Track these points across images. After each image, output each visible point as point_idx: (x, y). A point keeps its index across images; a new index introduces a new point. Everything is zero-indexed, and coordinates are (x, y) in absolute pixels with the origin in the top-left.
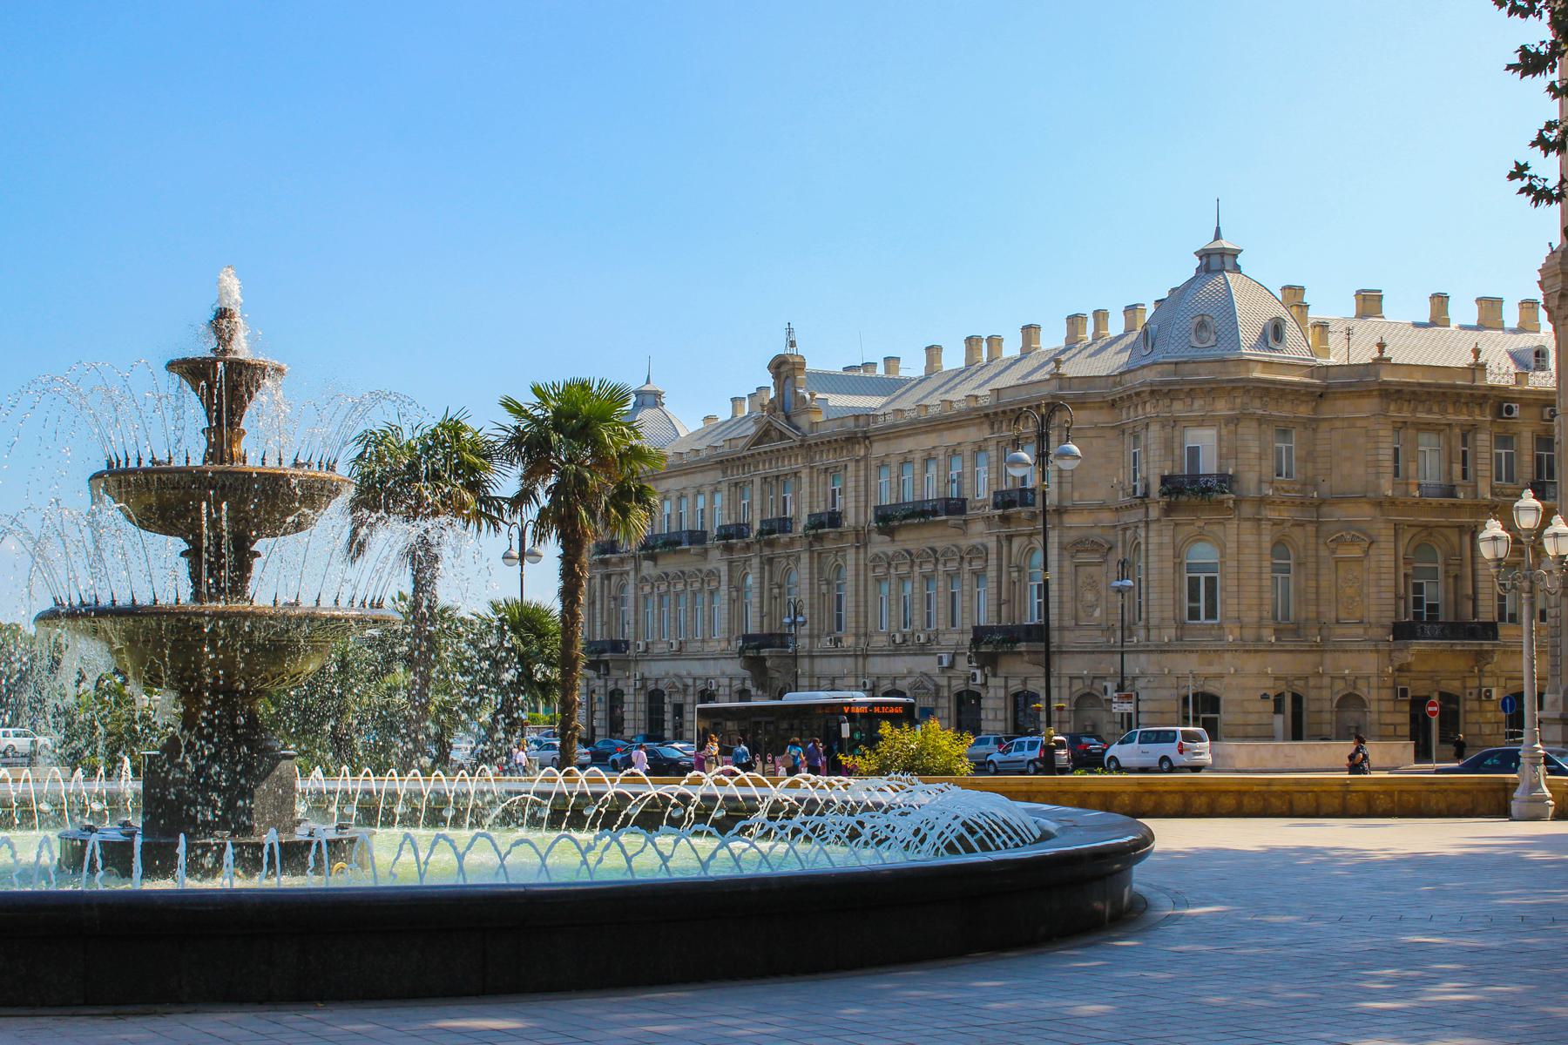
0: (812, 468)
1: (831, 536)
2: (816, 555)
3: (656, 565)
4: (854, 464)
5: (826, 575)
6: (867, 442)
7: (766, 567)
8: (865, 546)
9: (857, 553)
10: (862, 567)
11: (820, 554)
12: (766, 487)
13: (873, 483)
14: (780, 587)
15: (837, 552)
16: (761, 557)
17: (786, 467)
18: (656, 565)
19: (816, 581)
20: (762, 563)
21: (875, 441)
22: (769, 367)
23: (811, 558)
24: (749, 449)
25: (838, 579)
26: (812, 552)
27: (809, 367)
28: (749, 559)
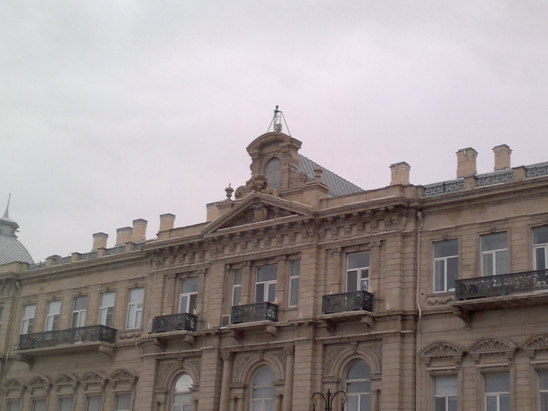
0: (319, 247)
1: (365, 320)
2: (320, 347)
3: (31, 368)
4: (399, 238)
5: (333, 372)
6: (419, 214)
7: (226, 364)
8: (415, 334)
9: (402, 343)
10: (409, 360)
11: (325, 346)
12: (231, 275)
13: (425, 261)
14: (245, 388)
15: (359, 342)
16: (220, 353)
17: (287, 245)
18: (31, 368)
19: (319, 377)
20: (221, 360)
21: (430, 213)
22: (249, 149)
23: (314, 350)
24: (214, 232)
25: (348, 379)
26: (315, 342)
27: (300, 152)
28: (199, 355)
